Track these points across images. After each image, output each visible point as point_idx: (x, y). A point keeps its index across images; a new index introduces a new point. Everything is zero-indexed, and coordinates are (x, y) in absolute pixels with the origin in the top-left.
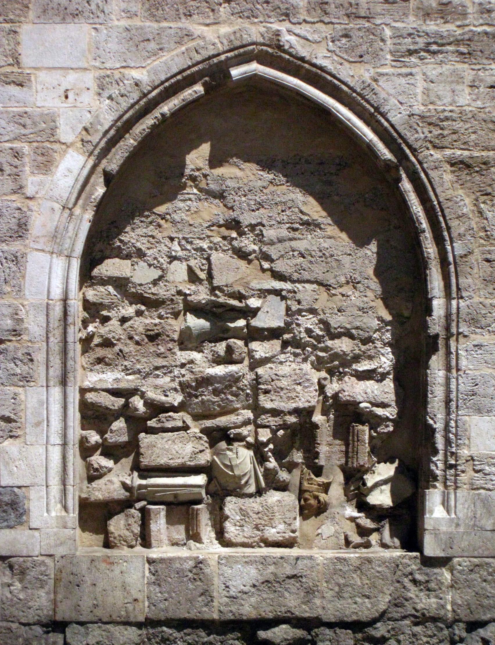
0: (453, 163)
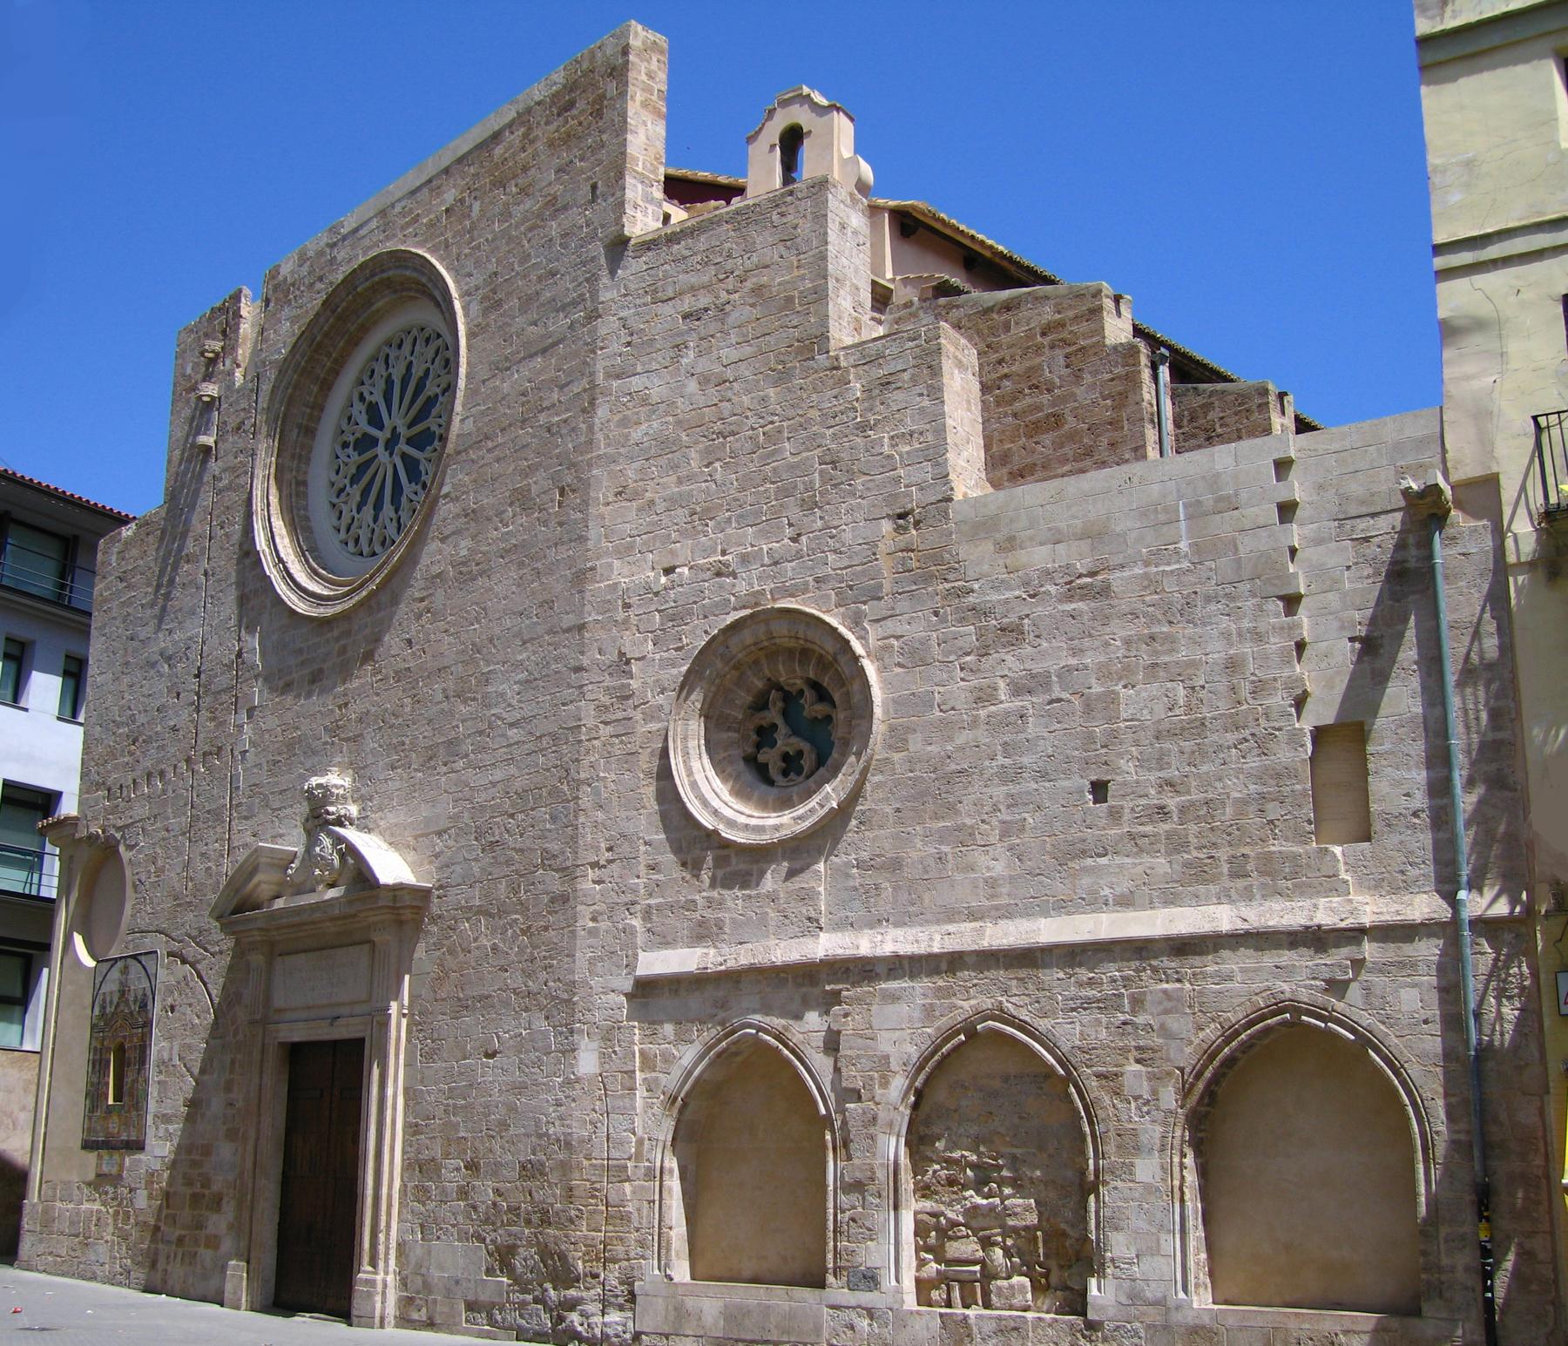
0: (1099, 1076)
